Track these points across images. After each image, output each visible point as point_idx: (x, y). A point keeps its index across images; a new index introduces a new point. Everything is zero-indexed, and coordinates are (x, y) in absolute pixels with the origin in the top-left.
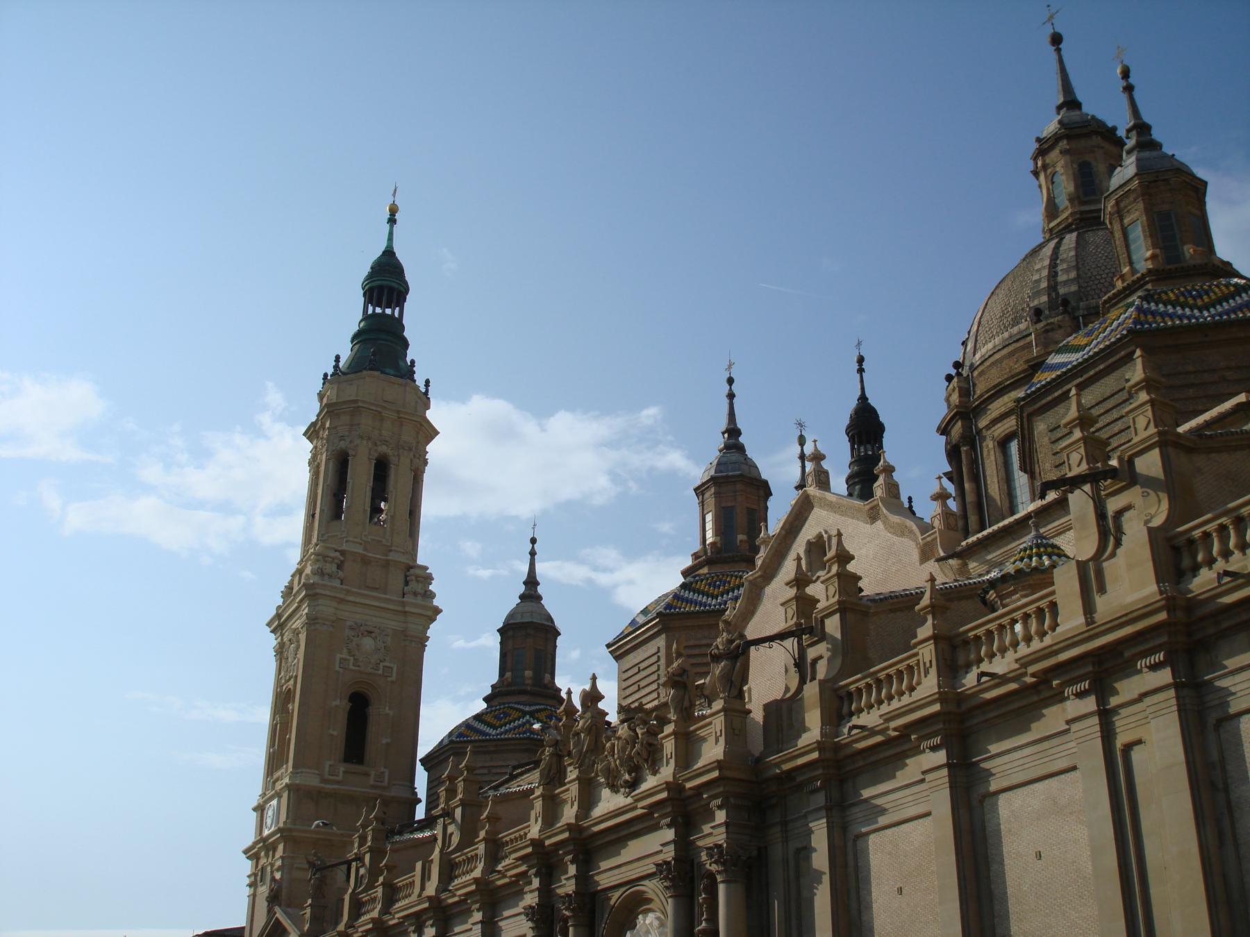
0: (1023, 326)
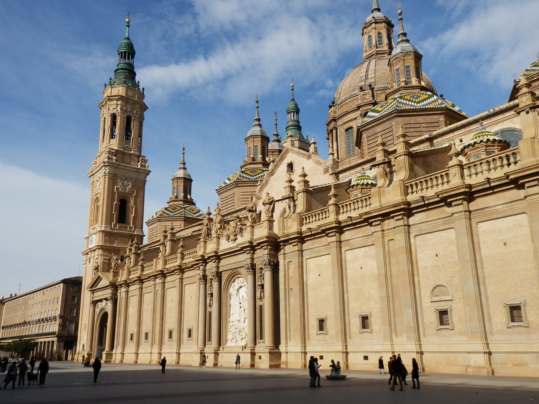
0: (356, 92)
